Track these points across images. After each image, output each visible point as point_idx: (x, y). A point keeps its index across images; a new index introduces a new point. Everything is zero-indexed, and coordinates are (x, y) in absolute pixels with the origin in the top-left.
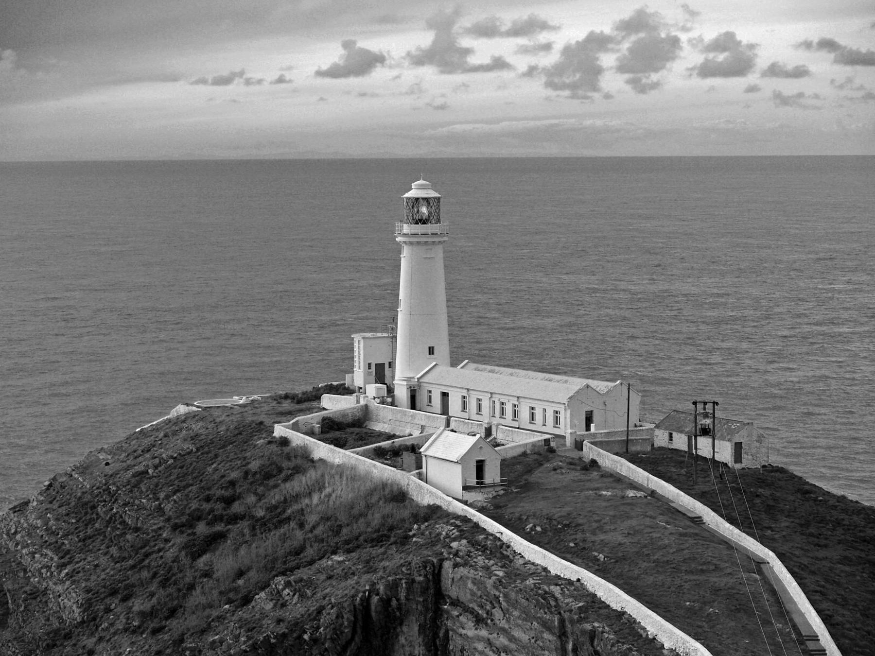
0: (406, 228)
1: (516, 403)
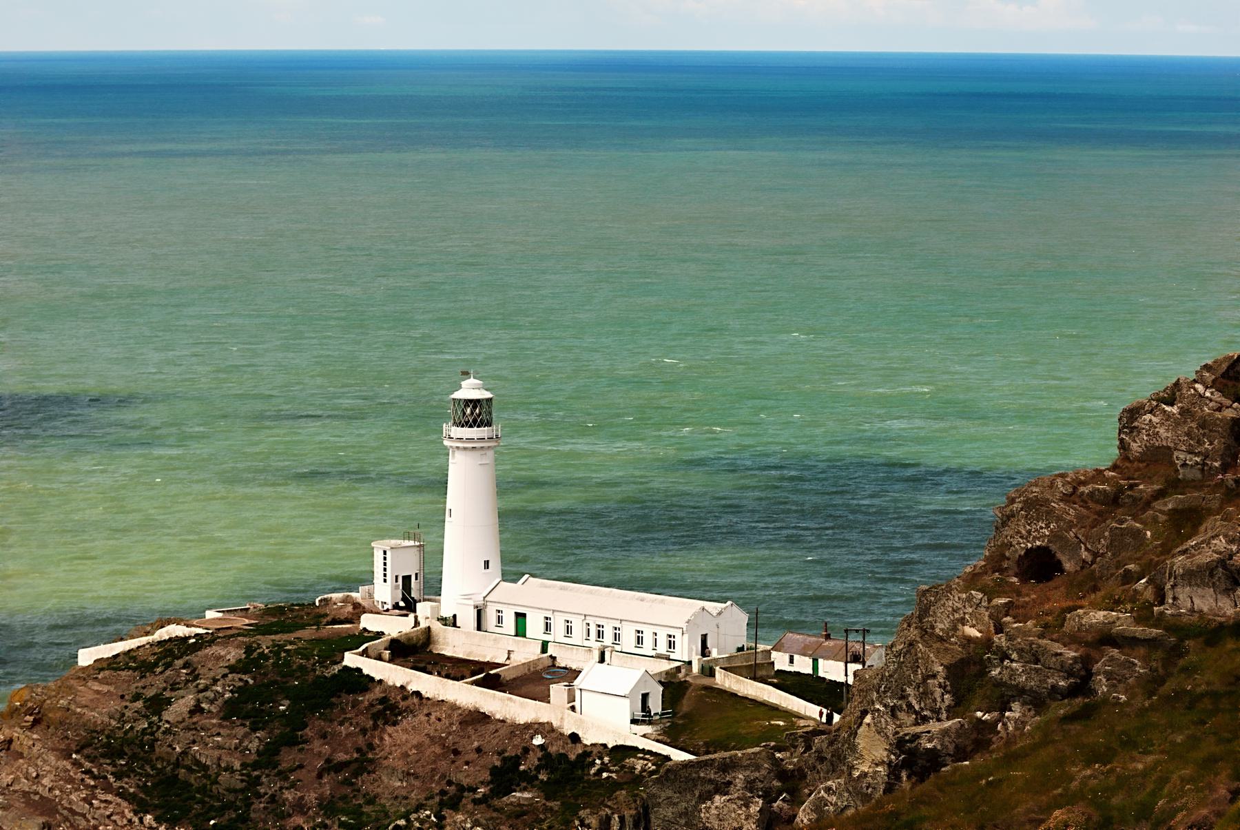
0: (457, 432)
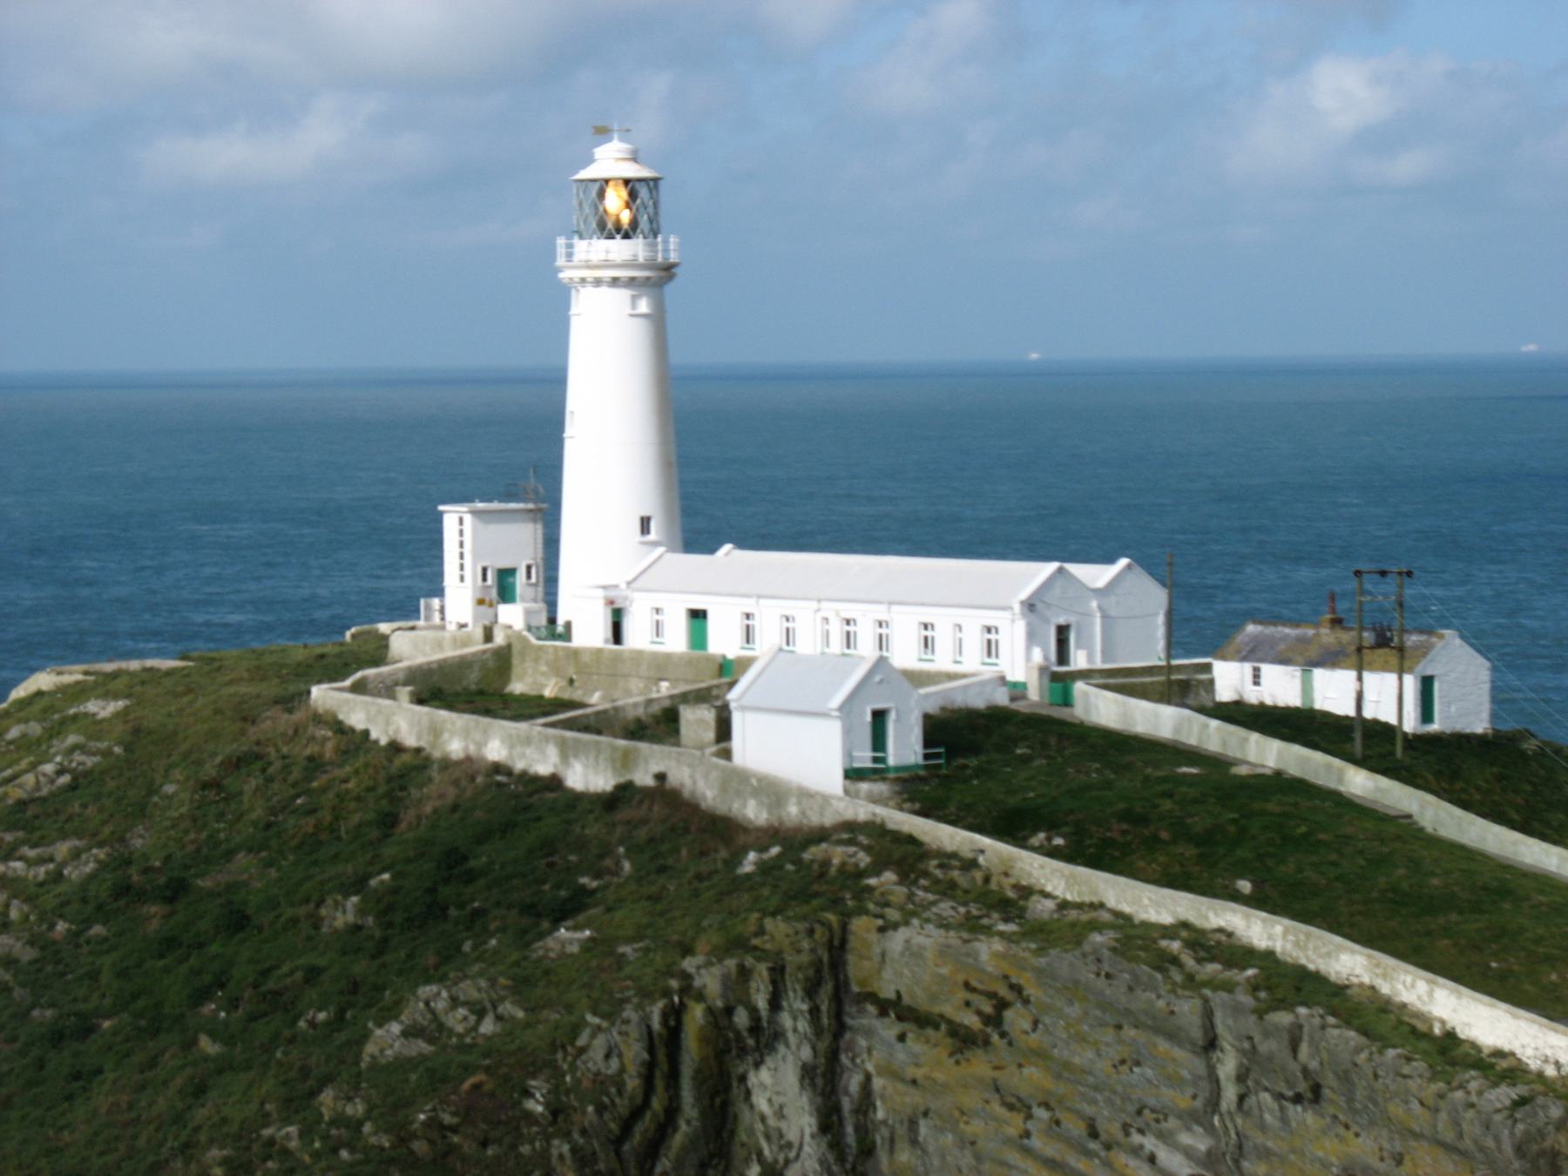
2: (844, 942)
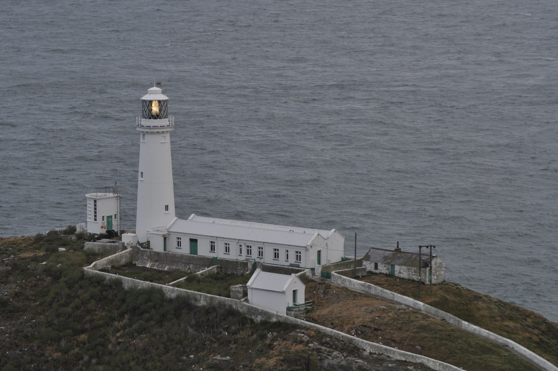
0: (146, 122)
1: (261, 246)
2: (308, 362)
